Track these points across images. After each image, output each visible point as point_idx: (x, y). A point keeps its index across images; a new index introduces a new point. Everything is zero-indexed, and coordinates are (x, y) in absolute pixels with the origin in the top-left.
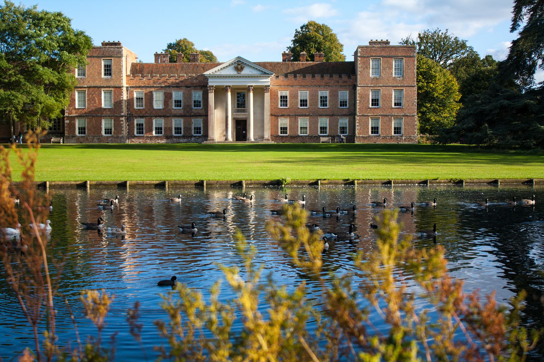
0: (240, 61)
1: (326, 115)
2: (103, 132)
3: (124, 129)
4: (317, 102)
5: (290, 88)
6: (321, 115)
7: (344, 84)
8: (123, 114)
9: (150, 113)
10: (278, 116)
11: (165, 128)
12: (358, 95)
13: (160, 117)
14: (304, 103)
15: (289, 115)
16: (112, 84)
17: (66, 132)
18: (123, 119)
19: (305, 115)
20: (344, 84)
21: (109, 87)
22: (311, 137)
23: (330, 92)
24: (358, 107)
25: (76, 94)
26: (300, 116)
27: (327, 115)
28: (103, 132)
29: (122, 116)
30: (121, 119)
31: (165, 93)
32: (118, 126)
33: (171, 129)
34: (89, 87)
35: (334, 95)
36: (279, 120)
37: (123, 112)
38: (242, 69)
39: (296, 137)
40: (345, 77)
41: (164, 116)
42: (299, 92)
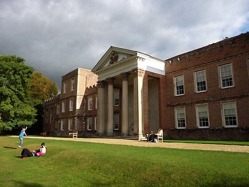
0: (115, 51)
1: (231, 98)
3: (76, 125)
4: (217, 81)
6: (224, 99)
8: (76, 115)
10: (174, 106)
14: (202, 85)
15: (185, 104)
18: (75, 118)
19: (204, 101)
22: (212, 130)
23: (234, 65)
26: (197, 103)
27: (234, 98)
36: (176, 110)
38: (116, 58)
39: (194, 130)
42: (195, 74)
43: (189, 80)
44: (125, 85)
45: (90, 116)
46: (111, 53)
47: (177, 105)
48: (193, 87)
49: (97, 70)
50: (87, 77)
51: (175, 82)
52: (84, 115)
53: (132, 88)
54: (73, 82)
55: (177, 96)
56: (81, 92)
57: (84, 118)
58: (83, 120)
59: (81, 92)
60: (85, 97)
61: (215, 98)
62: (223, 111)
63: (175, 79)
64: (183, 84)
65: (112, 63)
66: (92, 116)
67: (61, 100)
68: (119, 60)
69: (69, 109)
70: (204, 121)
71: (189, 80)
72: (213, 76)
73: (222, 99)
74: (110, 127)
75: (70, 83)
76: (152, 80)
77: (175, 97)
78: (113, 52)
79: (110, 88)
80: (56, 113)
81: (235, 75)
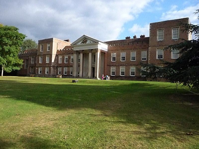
2: (46, 73)
3: (52, 71)
5: (117, 51)
7: (145, 47)
8: (52, 65)
9: (60, 66)
11: (68, 71)
12: (149, 52)
13: (66, 67)
14: (123, 58)
15: (116, 65)
16: (49, 53)
17: (36, 73)
18: (51, 67)
19: (124, 65)
20: (145, 47)
21: (48, 54)
22: (126, 77)
24: (149, 59)
25: (40, 58)
26: (121, 65)
28: (46, 73)
29: (51, 66)
30: (51, 67)
31: (68, 56)
32: (50, 70)
33: (69, 72)
34: (43, 55)
35: (139, 54)
36: (111, 68)
37: (51, 65)
38: (86, 41)
39: (118, 77)
40: (145, 44)
41: (68, 67)
42: (121, 53)
43: (118, 55)
44: (90, 55)
45: (61, 67)
46: (83, 38)
47: (112, 66)
48: (120, 59)
49: (74, 45)
50: (58, 43)
51: (112, 55)
52: (56, 66)
53: (94, 56)
54: (48, 45)
55: (112, 62)
56: (54, 53)
57: (56, 68)
58: (55, 68)
59: (54, 53)
60: (57, 56)
61: (128, 64)
62: (130, 70)
63: (112, 54)
64: (115, 56)
65: (83, 43)
66: (61, 67)
67: (38, 55)
68: (87, 43)
69: (46, 61)
70: (123, 73)
71: (118, 55)
72: (128, 55)
73: (131, 65)
74: (90, 74)
75: (46, 46)
76: (103, 53)
77: (111, 62)
78: (84, 38)
79: (81, 55)
80: (31, 63)
81: (136, 56)
